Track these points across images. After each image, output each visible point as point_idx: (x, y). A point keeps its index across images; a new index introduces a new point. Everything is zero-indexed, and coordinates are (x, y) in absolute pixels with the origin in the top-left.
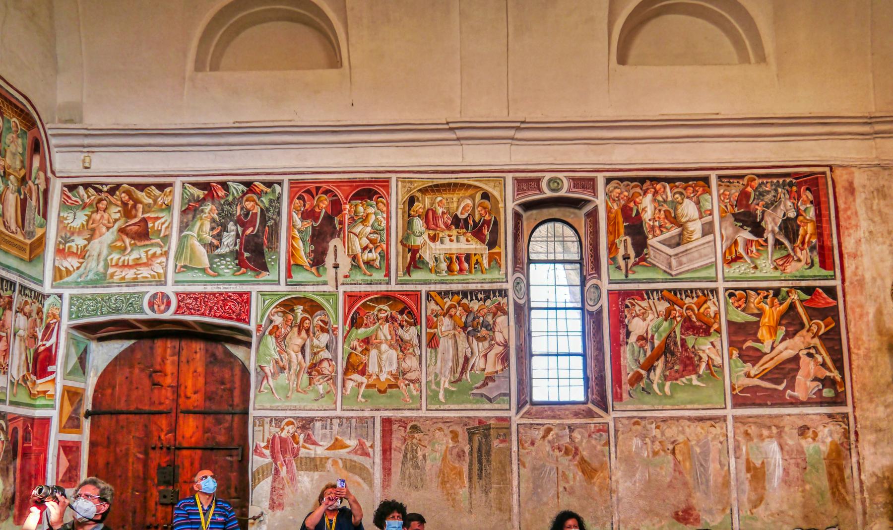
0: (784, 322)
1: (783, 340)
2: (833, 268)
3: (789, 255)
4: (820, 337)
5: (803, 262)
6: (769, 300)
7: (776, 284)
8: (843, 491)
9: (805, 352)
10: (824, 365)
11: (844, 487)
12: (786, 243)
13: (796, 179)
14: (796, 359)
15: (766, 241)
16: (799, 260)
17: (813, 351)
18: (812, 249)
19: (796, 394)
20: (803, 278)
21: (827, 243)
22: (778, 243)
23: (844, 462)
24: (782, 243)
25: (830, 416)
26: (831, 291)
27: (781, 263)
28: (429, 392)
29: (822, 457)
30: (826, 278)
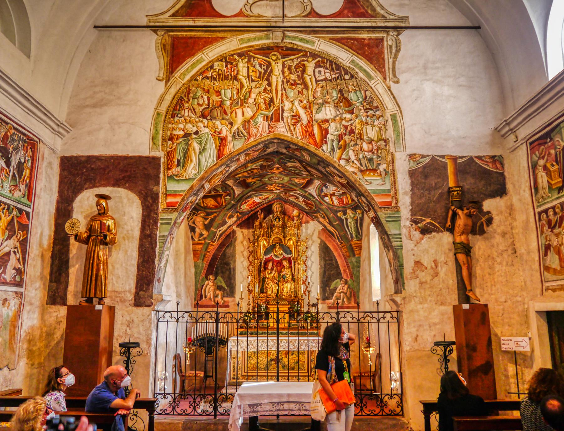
0: (9, 228)
1: (6, 240)
2: (31, 202)
3: (16, 185)
4: (20, 242)
5: (21, 193)
6: (5, 211)
7: (9, 202)
8: (13, 342)
9: (13, 250)
10: (19, 260)
11: (14, 340)
12: (17, 177)
13: (28, 139)
14: (8, 254)
15: (10, 171)
16: (20, 191)
17: (16, 250)
18: (26, 186)
19: (5, 277)
20: (19, 202)
21: (32, 185)
22: (14, 175)
23: (16, 323)
24: (16, 177)
25: (16, 293)
26: (28, 214)
27: (13, 189)
28: (249, 365)
29: (9, 320)
30: (24, 204)
